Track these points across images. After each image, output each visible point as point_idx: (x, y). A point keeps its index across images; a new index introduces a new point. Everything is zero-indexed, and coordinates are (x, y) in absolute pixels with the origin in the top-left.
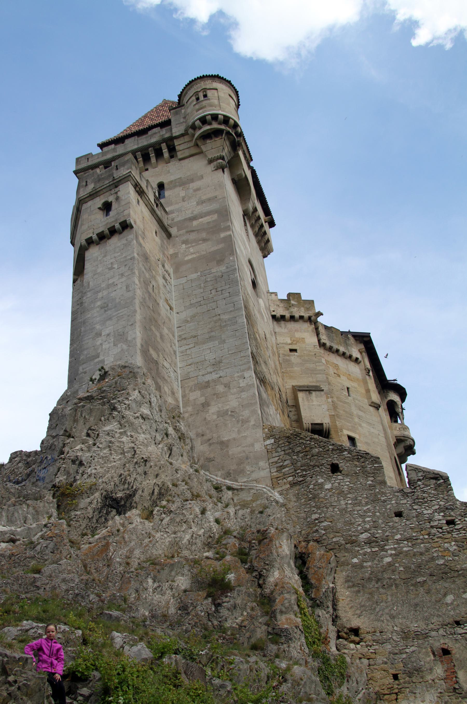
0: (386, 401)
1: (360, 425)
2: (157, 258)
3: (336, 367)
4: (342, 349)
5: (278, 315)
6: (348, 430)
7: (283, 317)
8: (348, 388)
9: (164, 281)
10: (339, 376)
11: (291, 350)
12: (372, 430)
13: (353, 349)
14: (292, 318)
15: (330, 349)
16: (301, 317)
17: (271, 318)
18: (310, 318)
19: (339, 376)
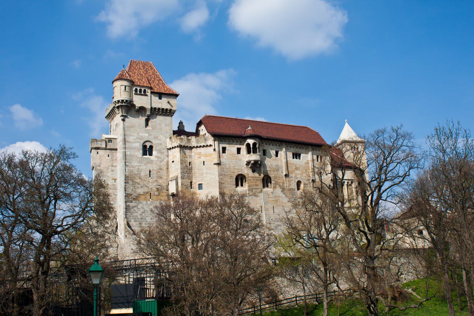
0: (245, 145)
1: (206, 177)
2: (108, 166)
3: (200, 153)
4: (202, 145)
5: (169, 148)
6: (199, 182)
7: (170, 149)
8: (204, 162)
9: (112, 172)
10: (200, 158)
11: (173, 162)
12: (212, 176)
13: (209, 141)
14: (173, 148)
15: (197, 147)
16: (175, 147)
17: (166, 151)
18: (178, 146)
19: (200, 158)
